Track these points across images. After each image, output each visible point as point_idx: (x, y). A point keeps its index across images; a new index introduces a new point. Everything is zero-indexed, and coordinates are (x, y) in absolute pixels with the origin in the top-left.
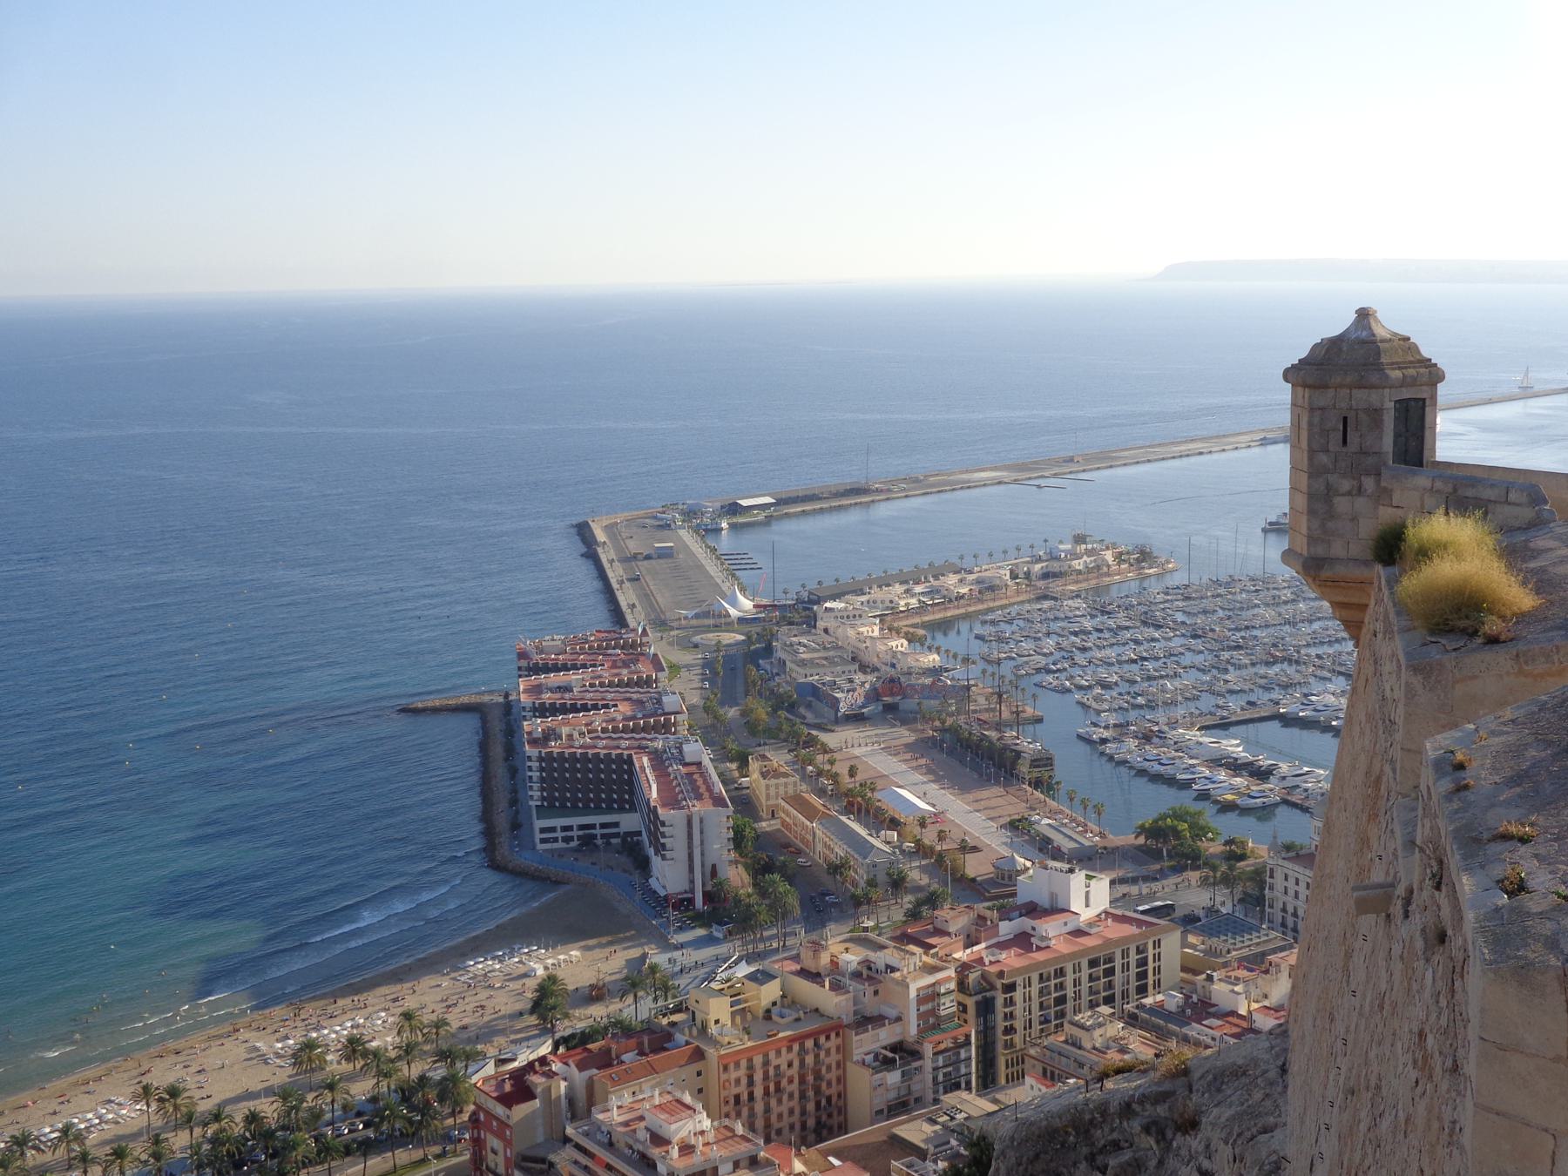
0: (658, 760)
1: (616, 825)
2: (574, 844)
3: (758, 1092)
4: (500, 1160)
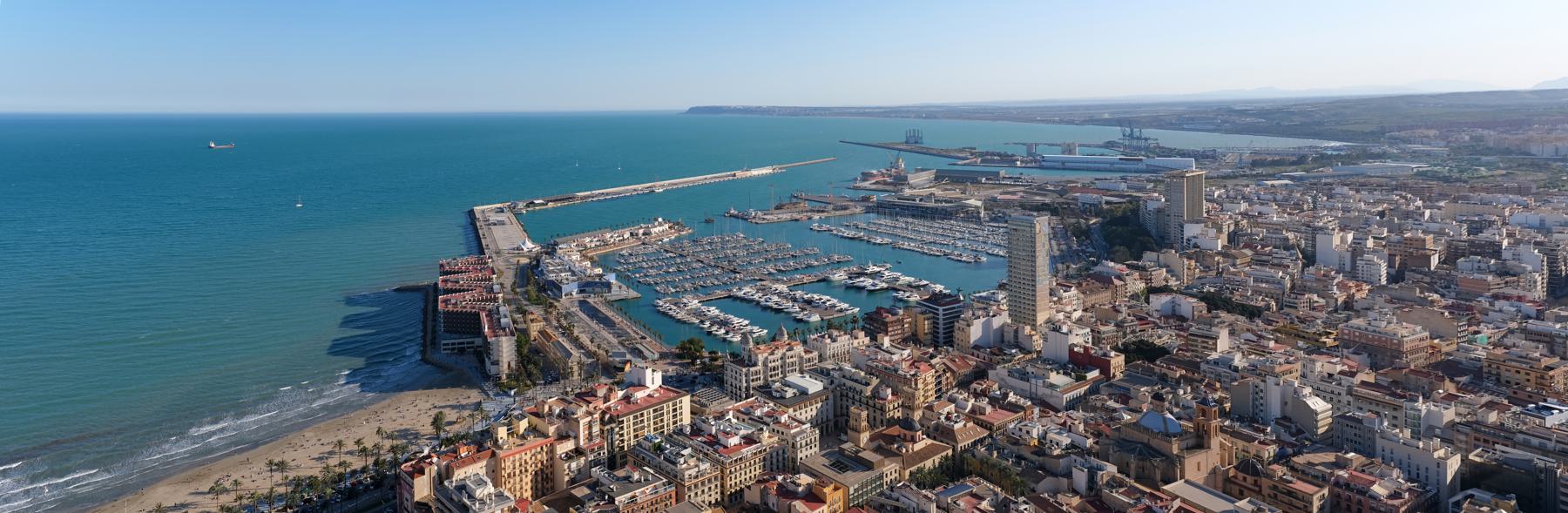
0: (490, 314)
1: (473, 343)
2: (456, 351)
3: (517, 472)
4: (409, 504)
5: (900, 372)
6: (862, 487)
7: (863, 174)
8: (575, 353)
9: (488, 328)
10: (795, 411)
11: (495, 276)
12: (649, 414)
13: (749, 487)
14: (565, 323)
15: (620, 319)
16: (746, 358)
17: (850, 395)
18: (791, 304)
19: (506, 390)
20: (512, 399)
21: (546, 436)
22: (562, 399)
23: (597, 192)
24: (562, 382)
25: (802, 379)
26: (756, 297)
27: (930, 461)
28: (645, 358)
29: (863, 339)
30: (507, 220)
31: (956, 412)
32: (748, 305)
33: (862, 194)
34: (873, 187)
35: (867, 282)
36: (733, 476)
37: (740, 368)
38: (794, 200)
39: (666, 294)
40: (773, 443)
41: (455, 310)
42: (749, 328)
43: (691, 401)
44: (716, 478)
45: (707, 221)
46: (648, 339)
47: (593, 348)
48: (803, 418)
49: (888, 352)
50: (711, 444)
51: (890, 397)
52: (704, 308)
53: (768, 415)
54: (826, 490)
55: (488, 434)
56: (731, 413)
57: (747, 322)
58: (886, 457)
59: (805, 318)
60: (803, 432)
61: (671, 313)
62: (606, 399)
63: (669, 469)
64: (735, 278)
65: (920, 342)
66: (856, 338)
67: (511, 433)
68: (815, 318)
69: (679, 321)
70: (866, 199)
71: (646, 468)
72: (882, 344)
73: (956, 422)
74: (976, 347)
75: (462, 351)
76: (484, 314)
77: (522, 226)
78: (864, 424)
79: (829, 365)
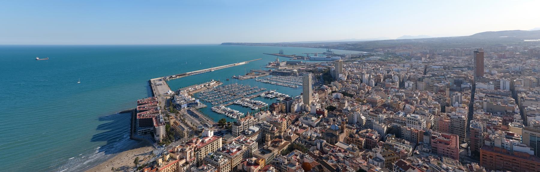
0: (156, 118)
1: (150, 129)
5: (278, 122)
6: (269, 158)
7: (269, 63)
8: (186, 128)
9: (156, 123)
10: (251, 138)
11: (158, 104)
12: (209, 146)
13: (239, 165)
14: (182, 118)
15: (201, 115)
16: (238, 123)
17: (266, 130)
18: (250, 104)
19: (162, 145)
20: (164, 148)
21: (175, 159)
22: (181, 145)
23: (193, 72)
24: (181, 139)
25: (253, 128)
26: (241, 103)
27: (285, 147)
28: (208, 127)
29: (269, 113)
30: (162, 83)
31: (291, 131)
32: (239, 106)
33: (269, 69)
34: (272, 67)
35: (270, 96)
36: (234, 162)
37: (236, 126)
38: (251, 72)
39: (215, 105)
40: (246, 149)
41: (143, 118)
42: (239, 113)
43: (222, 140)
44: (229, 164)
45: (227, 80)
46: (209, 121)
47: (192, 126)
48: (253, 140)
49: (275, 116)
50: (228, 153)
51: (276, 130)
52: (226, 108)
53: (244, 140)
54: (260, 161)
55: (155, 162)
56: (234, 141)
57: (238, 112)
58: (275, 148)
59: (254, 108)
60: (254, 144)
61: (216, 111)
62: (196, 143)
63: (215, 163)
64: (235, 98)
65: (283, 112)
66: (267, 113)
67: (163, 161)
68: (257, 108)
69: (219, 113)
70: (270, 71)
71: (209, 164)
72: (274, 114)
73: (291, 135)
74: (296, 112)
75: (146, 133)
76: (154, 118)
77: (168, 85)
78: (269, 139)
79: (260, 122)
